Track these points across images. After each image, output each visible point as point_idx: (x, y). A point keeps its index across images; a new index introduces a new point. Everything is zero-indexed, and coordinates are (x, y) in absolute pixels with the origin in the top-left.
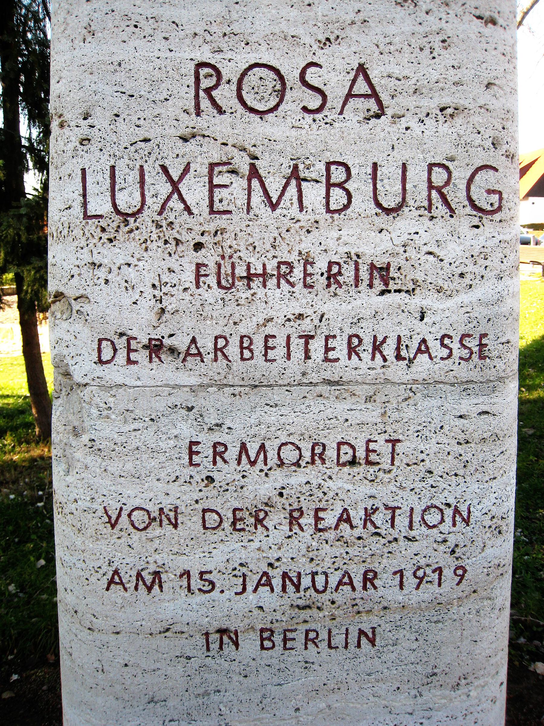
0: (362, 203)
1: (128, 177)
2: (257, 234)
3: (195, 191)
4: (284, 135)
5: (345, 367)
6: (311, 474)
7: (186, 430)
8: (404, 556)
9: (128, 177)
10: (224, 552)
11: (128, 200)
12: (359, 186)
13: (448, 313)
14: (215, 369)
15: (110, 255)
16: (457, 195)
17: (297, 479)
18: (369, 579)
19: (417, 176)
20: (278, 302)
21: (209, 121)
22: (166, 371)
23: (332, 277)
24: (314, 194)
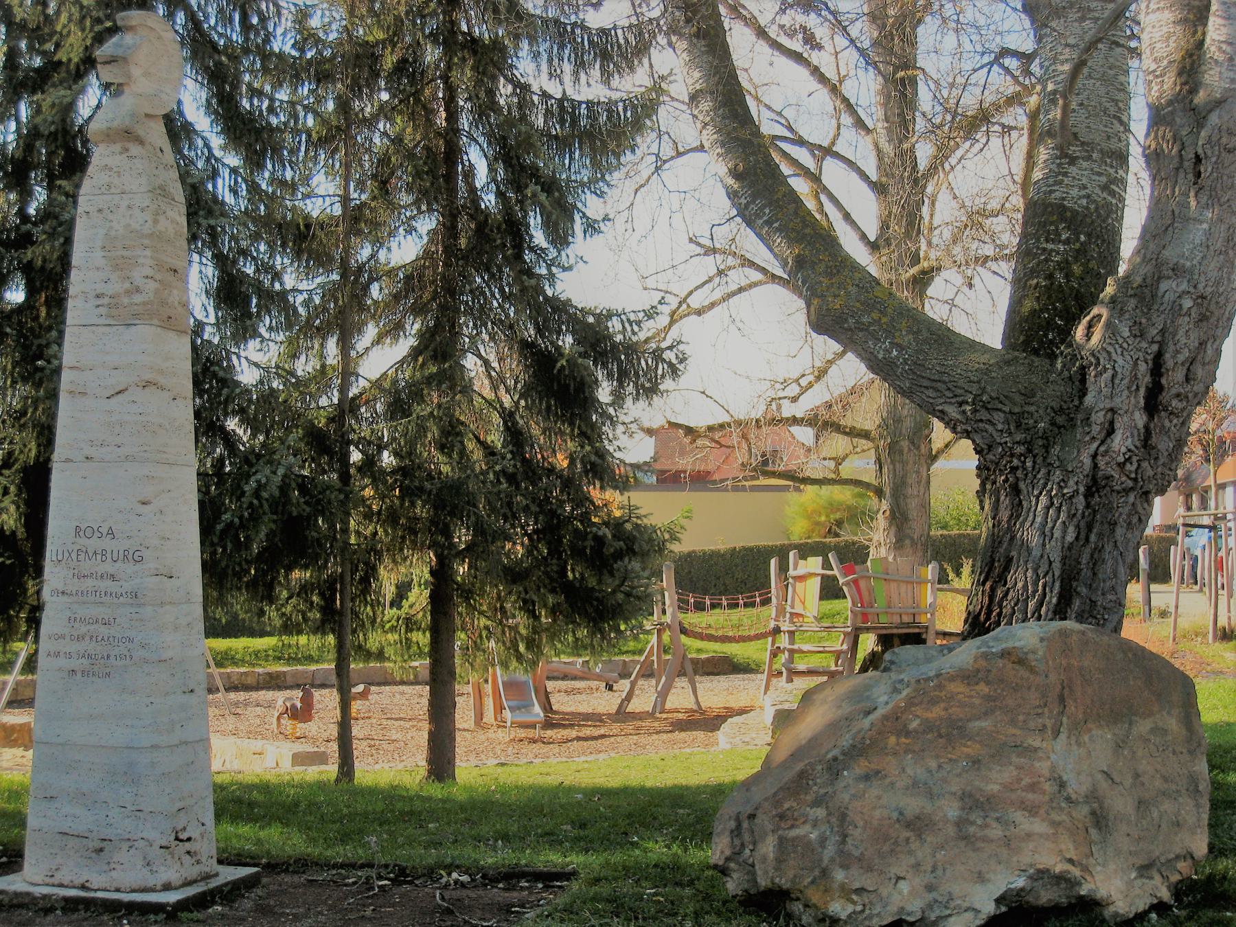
0: (109, 559)
1: (60, 552)
2: (87, 566)
3: (74, 556)
4: (94, 544)
5: (104, 599)
6: (95, 626)
7: (68, 613)
8: (116, 651)
9: (60, 552)
10: (74, 647)
11: (60, 558)
12: (109, 555)
13: (127, 586)
14: (75, 598)
15: (56, 570)
16: (130, 557)
17: (92, 627)
18: (108, 657)
19: (121, 553)
20: (90, 583)
21: (78, 539)
22: (65, 598)
23: (102, 577)
24: (99, 557)
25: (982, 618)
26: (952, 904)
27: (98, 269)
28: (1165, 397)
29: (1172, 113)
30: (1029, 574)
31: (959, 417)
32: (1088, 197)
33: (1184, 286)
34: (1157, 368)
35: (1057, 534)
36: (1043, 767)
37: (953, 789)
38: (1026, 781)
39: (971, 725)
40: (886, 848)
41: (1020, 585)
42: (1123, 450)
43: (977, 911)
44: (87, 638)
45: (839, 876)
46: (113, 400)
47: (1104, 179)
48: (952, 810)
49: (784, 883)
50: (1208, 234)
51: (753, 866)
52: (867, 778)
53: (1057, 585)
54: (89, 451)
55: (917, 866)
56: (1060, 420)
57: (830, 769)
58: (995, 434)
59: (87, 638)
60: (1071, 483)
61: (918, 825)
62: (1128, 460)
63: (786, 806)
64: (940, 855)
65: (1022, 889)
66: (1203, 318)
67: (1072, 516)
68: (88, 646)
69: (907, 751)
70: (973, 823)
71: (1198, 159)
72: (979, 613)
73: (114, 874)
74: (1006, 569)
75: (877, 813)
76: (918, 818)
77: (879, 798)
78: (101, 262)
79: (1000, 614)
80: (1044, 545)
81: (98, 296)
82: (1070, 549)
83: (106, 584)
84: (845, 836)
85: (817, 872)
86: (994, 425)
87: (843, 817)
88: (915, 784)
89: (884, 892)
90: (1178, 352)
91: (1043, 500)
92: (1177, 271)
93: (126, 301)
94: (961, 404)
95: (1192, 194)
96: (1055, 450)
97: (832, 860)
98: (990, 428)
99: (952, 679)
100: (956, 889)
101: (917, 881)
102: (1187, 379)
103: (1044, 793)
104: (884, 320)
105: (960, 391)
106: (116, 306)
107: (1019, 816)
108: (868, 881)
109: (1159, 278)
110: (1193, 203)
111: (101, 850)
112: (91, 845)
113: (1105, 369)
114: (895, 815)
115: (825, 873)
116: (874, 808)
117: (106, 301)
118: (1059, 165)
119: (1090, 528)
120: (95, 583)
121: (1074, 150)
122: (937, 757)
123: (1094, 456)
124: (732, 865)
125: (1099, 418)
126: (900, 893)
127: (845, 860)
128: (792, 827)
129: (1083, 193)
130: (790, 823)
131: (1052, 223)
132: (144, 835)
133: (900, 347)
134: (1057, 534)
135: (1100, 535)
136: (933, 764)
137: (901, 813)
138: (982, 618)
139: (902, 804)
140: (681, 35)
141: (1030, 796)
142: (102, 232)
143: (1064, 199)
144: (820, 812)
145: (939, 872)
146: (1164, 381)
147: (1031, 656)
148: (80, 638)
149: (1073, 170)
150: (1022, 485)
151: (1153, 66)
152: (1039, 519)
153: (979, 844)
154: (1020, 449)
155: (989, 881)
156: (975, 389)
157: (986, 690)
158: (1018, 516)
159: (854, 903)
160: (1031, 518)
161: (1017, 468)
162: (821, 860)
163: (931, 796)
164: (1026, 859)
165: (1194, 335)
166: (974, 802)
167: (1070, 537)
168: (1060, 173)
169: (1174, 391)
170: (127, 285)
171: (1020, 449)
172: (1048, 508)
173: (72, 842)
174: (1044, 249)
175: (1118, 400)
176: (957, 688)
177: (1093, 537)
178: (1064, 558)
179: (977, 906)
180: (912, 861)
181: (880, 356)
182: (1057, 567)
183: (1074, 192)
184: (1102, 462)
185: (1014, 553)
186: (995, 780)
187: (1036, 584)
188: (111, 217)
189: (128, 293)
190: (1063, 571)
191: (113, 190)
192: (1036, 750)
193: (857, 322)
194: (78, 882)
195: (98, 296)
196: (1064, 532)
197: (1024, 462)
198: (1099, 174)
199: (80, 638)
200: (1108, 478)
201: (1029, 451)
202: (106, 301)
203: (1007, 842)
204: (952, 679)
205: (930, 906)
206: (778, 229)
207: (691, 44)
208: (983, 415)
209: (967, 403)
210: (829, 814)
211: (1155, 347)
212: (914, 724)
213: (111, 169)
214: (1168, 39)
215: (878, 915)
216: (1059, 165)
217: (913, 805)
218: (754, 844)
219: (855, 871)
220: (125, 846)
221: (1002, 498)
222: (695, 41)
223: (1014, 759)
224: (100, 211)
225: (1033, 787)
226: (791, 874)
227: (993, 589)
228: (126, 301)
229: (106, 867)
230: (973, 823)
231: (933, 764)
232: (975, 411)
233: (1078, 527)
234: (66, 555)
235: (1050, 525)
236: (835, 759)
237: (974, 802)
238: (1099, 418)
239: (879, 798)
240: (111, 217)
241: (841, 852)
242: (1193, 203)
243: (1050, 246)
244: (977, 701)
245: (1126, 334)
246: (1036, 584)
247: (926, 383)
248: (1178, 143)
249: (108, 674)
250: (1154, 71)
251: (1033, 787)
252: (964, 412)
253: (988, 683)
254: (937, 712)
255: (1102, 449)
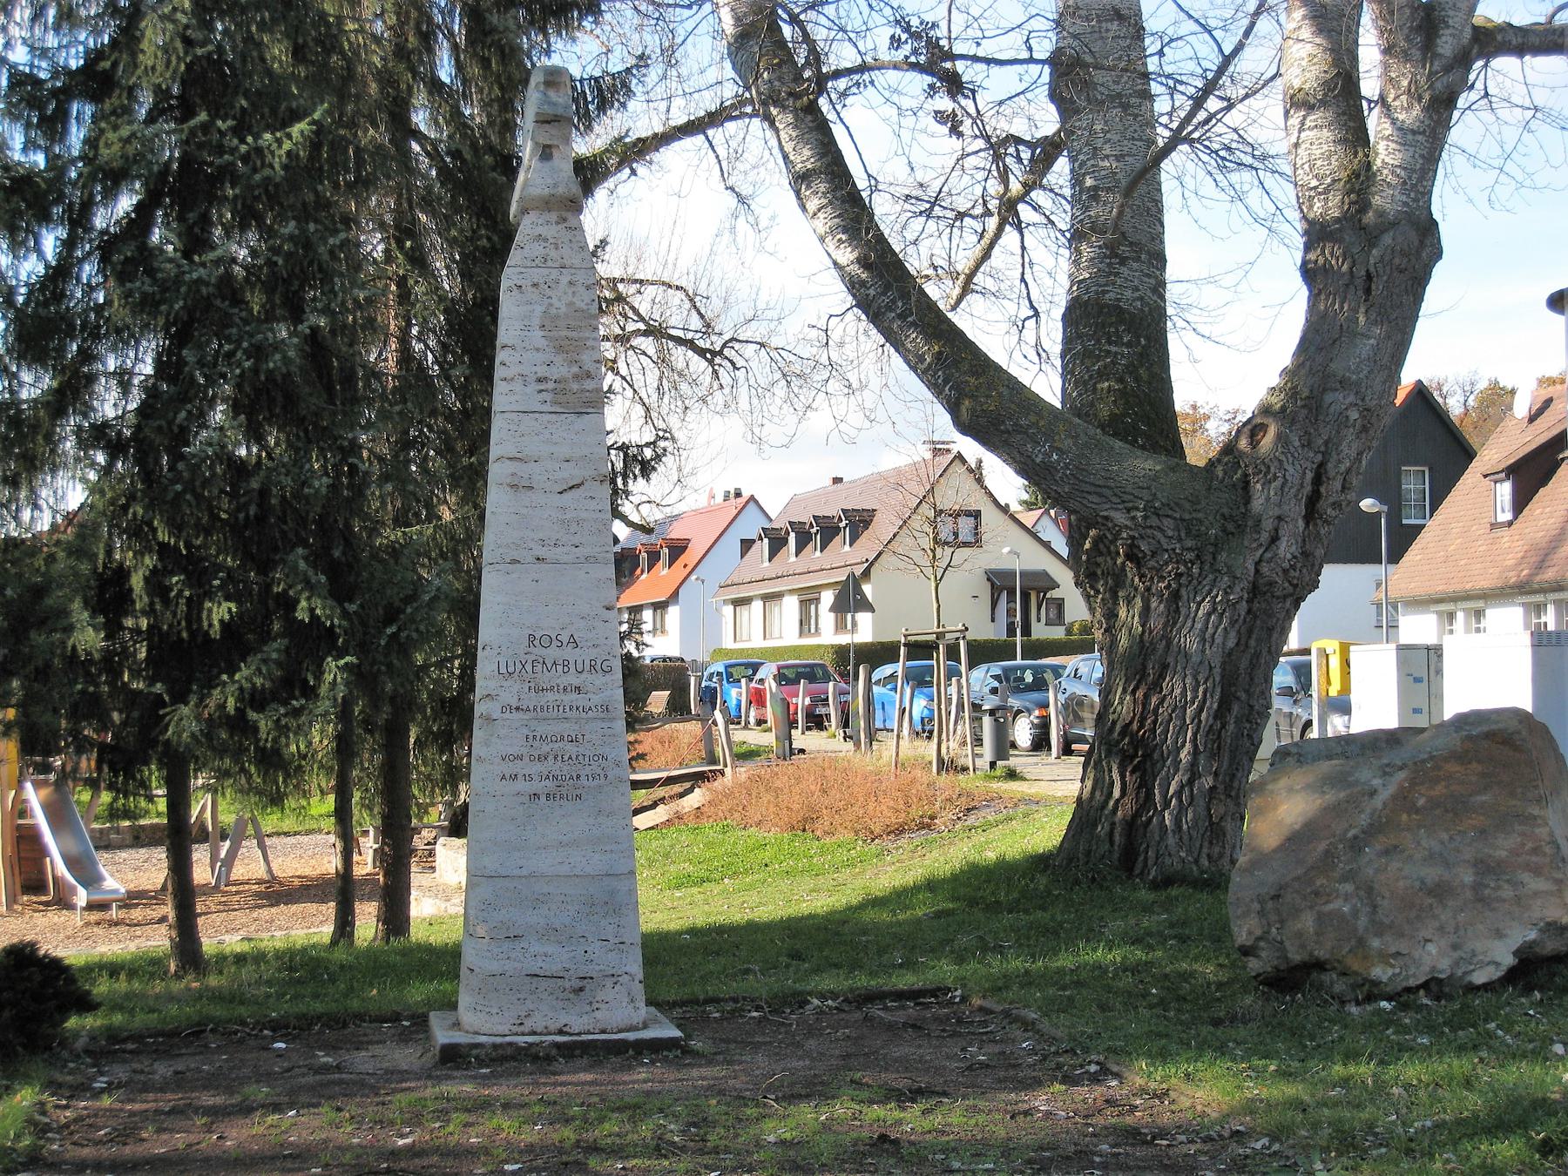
0: (572, 670)
1: (511, 664)
2: (545, 679)
3: (529, 667)
4: (552, 653)
5: (568, 714)
6: (560, 744)
7: (526, 731)
8: (588, 770)
9: (511, 664)
10: (536, 768)
11: (511, 669)
12: (572, 666)
13: (596, 699)
14: (533, 714)
15: (505, 684)
16: (598, 667)
17: (556, 746)
18: (578, 777)
19: (587, 663)
20: (550, 696)
21: (532, 649)
22: (520, 715)
23: (565, 690)
24: (560, 668)
25: (1135, 726)
26: (1475, 960)
27: (538, 350)
28: (1322, 505)
29: (1340, 230)
30: (1188, 681)
31: (1128, 523)
32: (1141, 299)
33: (1351, 399)
34: (1318, 480)
35: (1219, 639)
36: (1542, 832)
37: (1467, 857)
38: (1529, 845)
39: (1473, 799)
40: (1413, 914)
41: (1177, 691)
42: (1289, 556)
43: (1497, 964)
44: (551, 757)
45: (1376, 943)
46: (565, 495)
47: (1153, 281)
48: (1468, 877)
49: (1321, 953)
50: (1377, 349)
51: (1281, 943)
52: (1386, 852)
53: (1218, 690)
54: (542, 552)
55: (1441, 929)
56: (1230, 527)
57: (1352, 847)
58: (1163, 541)
59: (551, 757)
60: (1237, 589)
61: (1440, 892)
62: (1293, 567)
63: (1318, 883)
64: (1462, 917)
65: (1534, 941)
66: (1365, 429)
67: (1233, 623)
68: (550, 765)
69: (1419, 827)
70: (1487, 886)
71: (1369, 277)
72: (1131, 722)
73: (598, 1014)
74: (1162, 677)
75: (1401, 883)
76: (1438, 885)
77: (1400, 870)
78: (542, 343)
79: (1155, 722)
80: (1203, 651)
81: (539, 380)
82: (1230, 654)
83: (572, 697)
84: (1375, 907)
85: (1353, 942)
86: (1162, 531)
87: (1370, 890)
88: (1431, 856)
89: (1416, 954)
90: (1339, 462)
91: (1206, 606)
92: (1344, 383)
93: (575, 387)
94: (1129, 510)
95: (1362, 310)
96: (1223, 556)
97: (1366, 929)
98: (1159, 535)
99: (1446, 760)
100: (1478, 946)
101: (1443, 943)
102: (1343, 487)
103: (1545, 854)
104: (1042, 423)
105: (1126, 497)
106: (564, 392)
107: (1525, 877)
108: (1403, 946)
109: (1325, 390)
110: (1362, 319)
111: (581, 989)
112: (567, 984)
113: (1275, 478)
114: (1417, 884)
115: (1361, 942)
116: (1397, 880)
117: (551, 385)
118: (1110, 265)
119: (1250, 632)
120: (557, 696)
121: (1124, 249)
122: (1447, 830)
123: (1257, 564)
124: (1262, 944)
125: (1268, 525)
126: (1429, 954)
127: (1380, 929)
128: (1327, 902)
129: (1137, 294)
130: (1325, 899)
131: (1111, 325)
132: (627, 969)
133: (1060, 451)
134: (1219, 639)
135: (1259, 640)
136: (1445, 836)
137: (1423, 882)
138: (1135, 726)
139: (1422, 874)
140: (784, 108)
141: (1534, 859)
142: (539, 309)
143: (1119, 300)
144: (1348, 887)
145: (1462, 932)
146: (1322, 489)
147: (1516, 737)
148: (542, 758)
149: (1124, 270)
150: (1183, 592)
151: (1314, 183)
152: (1198, 626)
153: (1496, 905)
154: (1190, 556)
155: (1506, 936)
156: (1145, 494)
157: (1480, 768)
158: (1175, 623)
159: (1393, 966)
160: (1189, 624)
161: (1181, 575)
162: (1356, 930)
163: (1447, 865)
164: (1537, 914)
165: (1355, 446)
166: (1486, 868)
167: (1231, 643)
168: (1110, 273)
169: (1331, 500)
170: (575, 369)
171: (1190, 556)
172: (1209, 615)
173: (544, 984)
174: (1109, 352)
175: (1286, 508)
176: (1453, 767)
177: (1252, 643)
178: (1223, 663)
179: (1498, 959)
180: (1437, 924)
181: (1038, 460)
182: (1217, 671)
183: (1128, 293)
184: (1265, 569)
185: (1170, 660)
186: (1502, 847)
187: (1195, 690)
188: (548, 292)
189: (576, 377)
190: (1223, 677)
191: (549, 263)
192: (1535, 818)
193: (1015, 424)
194: (553, 1027)
195: (539, 380)
196: (1225, 637)
197: (1190, 569)
198: (1149, 276)
199: (542, 758)
200: (1271, 584)
201: (1198, 556)
202: (551, 385)
203: (1518, 899)
204: (1446, 760)
205: (1457, 964)
206: (913, 324)
207: (796, 118)
208: (1154, 521)
209: (1137, 509)
210: (1357, 888)
211: (1319, 457)
212: (1421, 802)
213: (546, 240)
214: (1329, 158)
215: (1414, 975)
216: (1110, 265)
217: (1432, 874)
218: (1282, 922)
219: (1388, 938)
220: (609, 982)
221: (1154, 605)
222: (801, 115)
223: (1517, 827)
224: (534, 285)
225: (1536, 851)
226: (1329, 945)
227: (1146, 697)
228: (575, 387)
229: (588, 1008)
230: (1487, 886)
231: (1445, 836)
232: (1145, 518)
233: (1239, 632)
234: (519, 666)
235: (1210, 630)
236: (1355, 837)
237: (1486, 868)
238: (1268, 525)
239: (1400, 870)
240: (548, 292)
241: (1372, 921)
242: (1362, 319)
243: (1113, 349)
244: (1474, 779)
245: (1297, 444)
246: (1195, 690)
247: (1088, 488)
248: (1349, 260)
249: (579, 797)
250: (1315, 188)
251: (1536, 851)
252: (1134, 518)
253: (1479, 762)
254: (1439, 790)
255: (1268, 555)
